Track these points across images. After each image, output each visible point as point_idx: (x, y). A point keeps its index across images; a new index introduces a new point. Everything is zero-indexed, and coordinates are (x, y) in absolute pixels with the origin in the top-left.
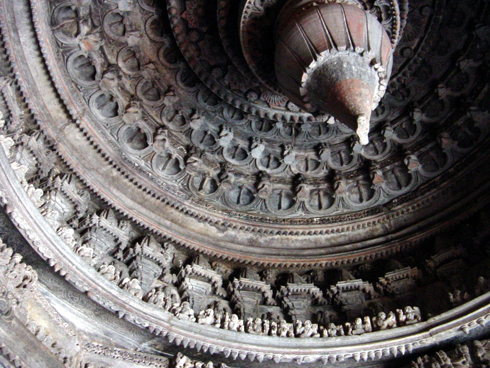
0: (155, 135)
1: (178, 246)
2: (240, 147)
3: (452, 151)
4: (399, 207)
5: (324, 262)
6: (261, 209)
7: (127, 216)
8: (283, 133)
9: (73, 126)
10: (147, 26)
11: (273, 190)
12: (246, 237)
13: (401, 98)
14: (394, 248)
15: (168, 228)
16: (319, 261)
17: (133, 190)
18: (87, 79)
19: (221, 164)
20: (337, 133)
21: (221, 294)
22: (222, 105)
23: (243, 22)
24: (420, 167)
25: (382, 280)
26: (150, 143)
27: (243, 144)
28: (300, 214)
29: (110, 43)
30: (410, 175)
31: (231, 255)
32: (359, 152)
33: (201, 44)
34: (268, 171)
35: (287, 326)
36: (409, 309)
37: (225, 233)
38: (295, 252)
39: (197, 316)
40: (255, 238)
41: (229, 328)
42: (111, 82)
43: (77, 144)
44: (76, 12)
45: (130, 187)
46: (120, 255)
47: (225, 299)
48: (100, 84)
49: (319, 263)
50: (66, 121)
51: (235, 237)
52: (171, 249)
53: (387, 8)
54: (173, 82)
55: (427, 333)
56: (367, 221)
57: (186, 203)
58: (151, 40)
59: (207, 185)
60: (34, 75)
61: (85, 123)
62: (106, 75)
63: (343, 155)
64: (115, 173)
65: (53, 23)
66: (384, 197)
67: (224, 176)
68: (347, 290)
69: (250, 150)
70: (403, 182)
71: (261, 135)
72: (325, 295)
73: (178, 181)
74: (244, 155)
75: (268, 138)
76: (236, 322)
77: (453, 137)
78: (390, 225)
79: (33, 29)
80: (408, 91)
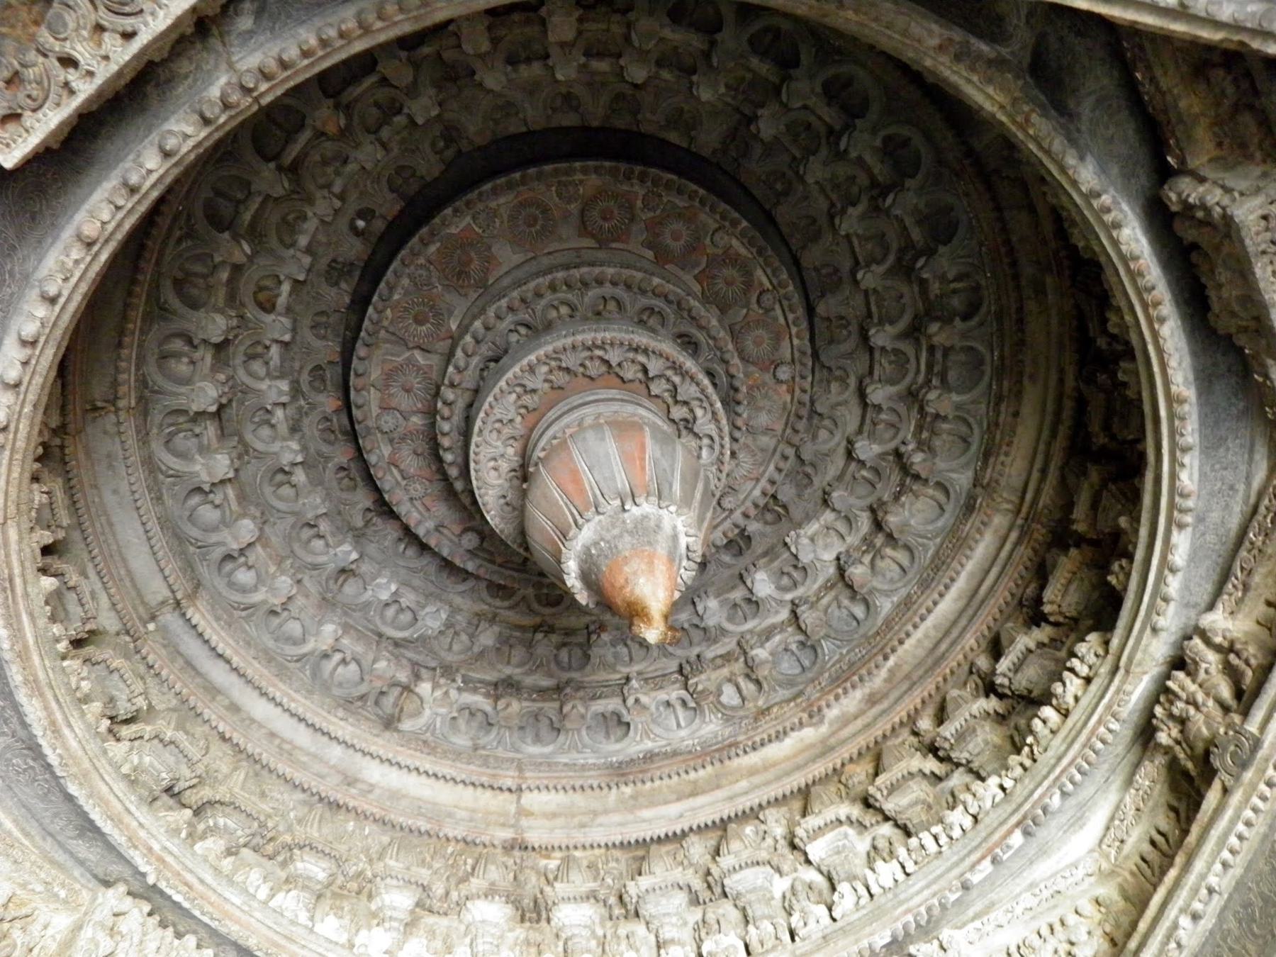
1: (777, 802)
2: (738, 601)
3: (964, 335)
4: (989, 470)
5: (972, 641)
6: (839, 647)
7: (683, 831)
10: (489, 600)
11: (826, 611)
12: (855, 702)
13: (845, 332)
14: (1036, 535)
16: (963, 648)
17: (669, 787)
18: (488, 732)
21: (873, 821)
24: (955, 398)
26: (627, 718)
28: (885, 606)
31: (851, 749)
32: (871, 454)
34: (800, 591)
36: (1081, 648)
37: (826, 721)
40: (867, 691)
42: (510, 710)
43: (552, 807)
44: (395, 684)
45: (660, 788)
49: (967, 648)
50: (514, 797)
51: (843, 714)
55: (1122, 672)
56: (973, 530)
57: (741, 738)
58: (510, 608)
59: (748, 687)
68: (1017, 668)
69: (751, 591)
71: (746, 560)
72: (1001, 696)
74: (754, 603)
75: (760, 551)
77: (947, 320)
78: (1009, 502)
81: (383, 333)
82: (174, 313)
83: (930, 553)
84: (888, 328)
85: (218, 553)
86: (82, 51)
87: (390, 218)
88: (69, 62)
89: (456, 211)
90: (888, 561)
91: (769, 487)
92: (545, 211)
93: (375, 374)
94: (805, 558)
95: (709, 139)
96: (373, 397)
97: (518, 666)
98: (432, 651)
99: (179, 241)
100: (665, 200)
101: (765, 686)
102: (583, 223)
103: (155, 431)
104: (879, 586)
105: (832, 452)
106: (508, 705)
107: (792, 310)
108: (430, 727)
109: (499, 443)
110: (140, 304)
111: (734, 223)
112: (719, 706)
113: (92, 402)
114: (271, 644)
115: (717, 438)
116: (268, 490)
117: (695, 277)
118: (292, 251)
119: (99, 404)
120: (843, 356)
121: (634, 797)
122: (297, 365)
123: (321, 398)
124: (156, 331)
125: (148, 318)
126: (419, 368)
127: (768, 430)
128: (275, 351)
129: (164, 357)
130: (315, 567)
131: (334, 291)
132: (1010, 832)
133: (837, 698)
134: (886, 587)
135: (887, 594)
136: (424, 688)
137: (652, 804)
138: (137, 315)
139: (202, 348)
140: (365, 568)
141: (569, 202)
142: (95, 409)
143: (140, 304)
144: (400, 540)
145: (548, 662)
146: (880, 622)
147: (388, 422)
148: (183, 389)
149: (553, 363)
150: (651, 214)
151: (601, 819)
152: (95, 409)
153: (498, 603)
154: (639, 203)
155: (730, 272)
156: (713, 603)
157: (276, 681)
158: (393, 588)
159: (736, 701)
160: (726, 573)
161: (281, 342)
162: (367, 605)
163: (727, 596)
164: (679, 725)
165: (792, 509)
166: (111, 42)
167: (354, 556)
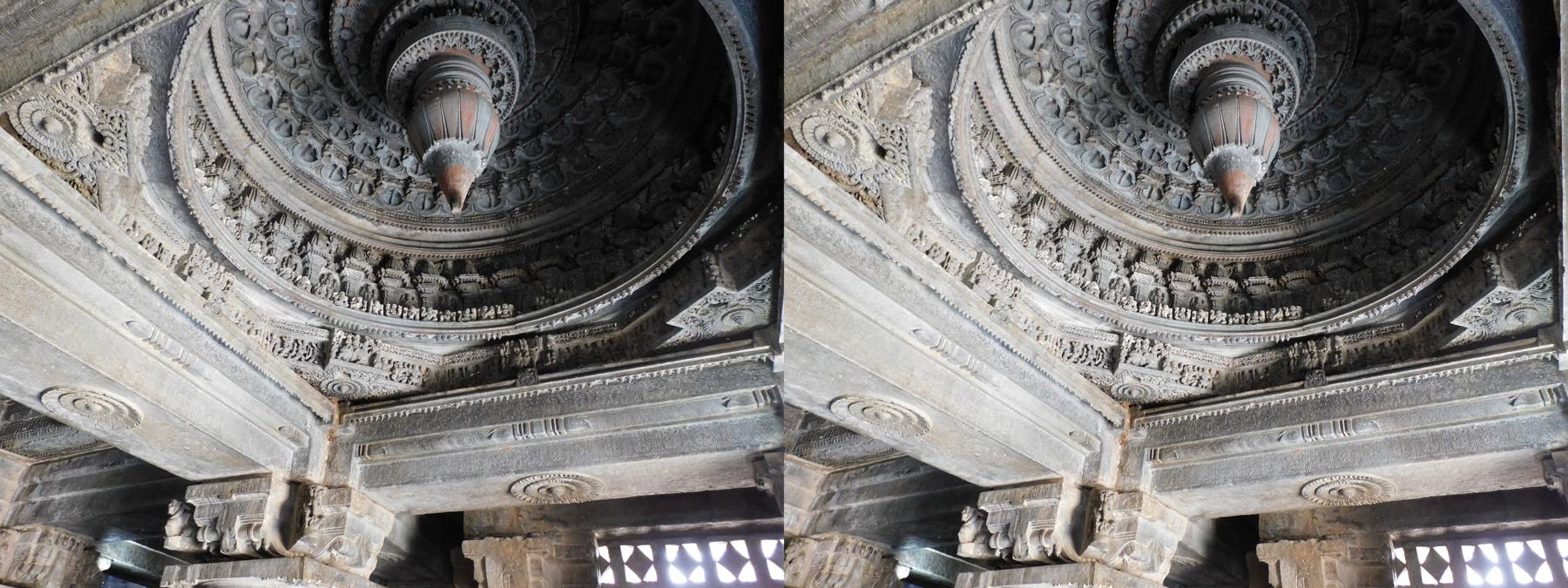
0: (323, 150)
15: (334, 225)
19: (377, 170)
25: (495, 276)
35: (415, 311)
38: (432, 245)
39: (350, 301)
41: (373, 312)
46: (296, 250)
47: (375, 282)
52: (336, 241)
54: (338, 103)
58: (318, 67)
60: (220, 107)
62: (282, 105)
64: (291, 181)
67: (378, 183)
76: (378, 306)
80: (540, 114)
101: (373, 196)
106: (286, 109)
121: (290, 186)
132: (432, 333)
137: (294, 194)
151: (273, 183)
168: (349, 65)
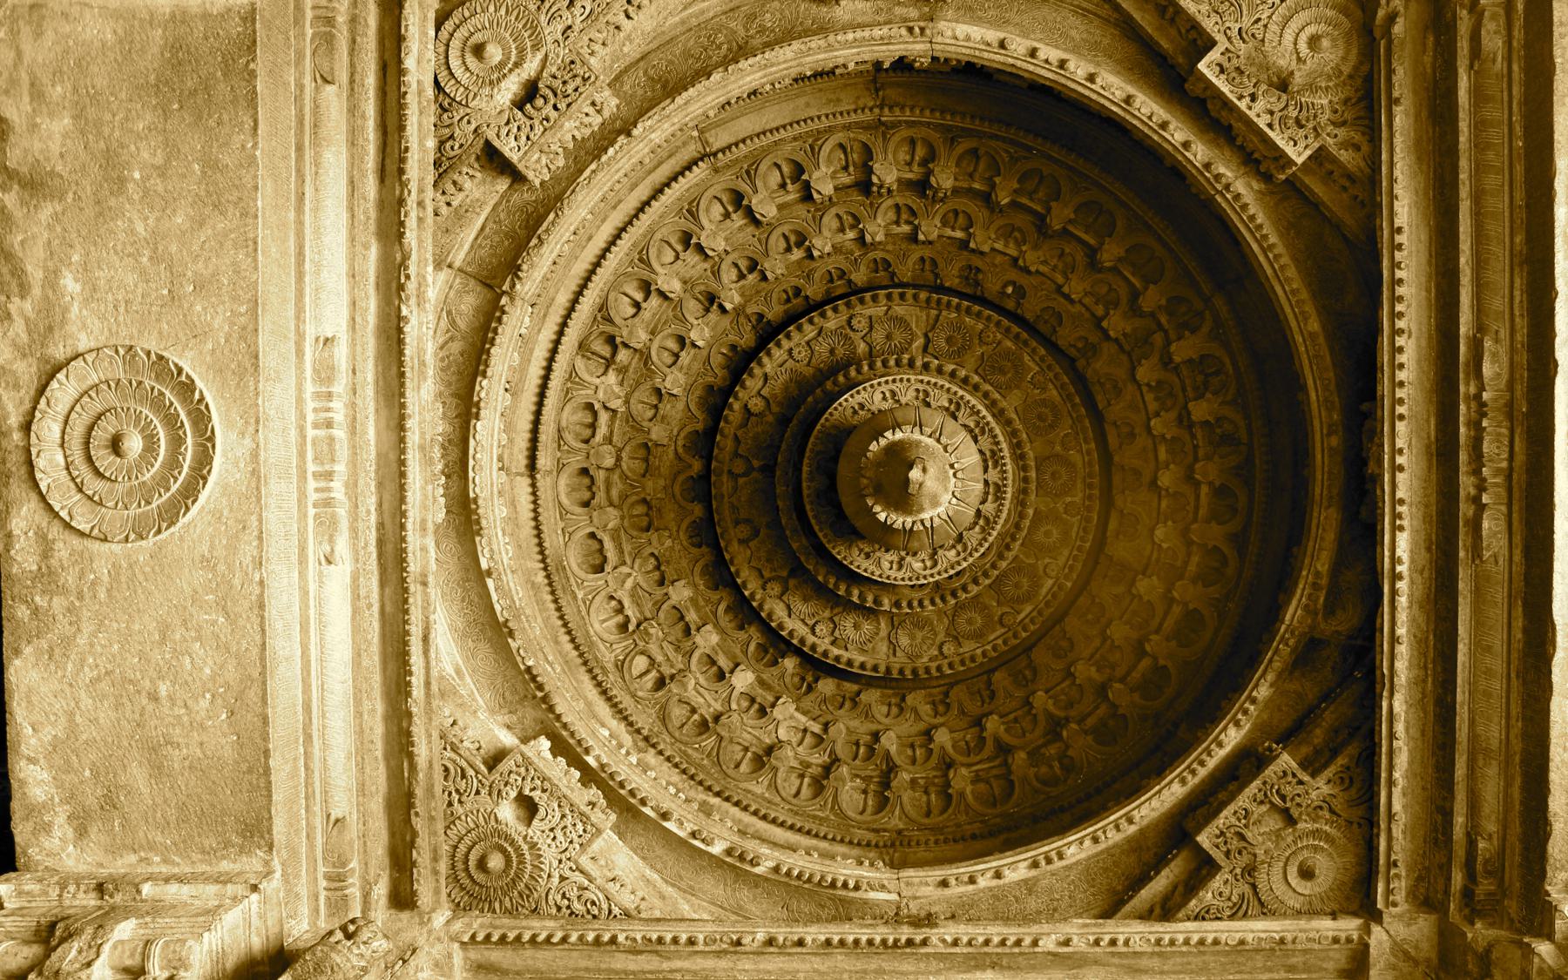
6: (709, 755)
8: (787, 680)
9: (529, 481)
10: (682, 435)
17: (548, 618)
20: (867, 716)
22: (724, 595)
23: (823, 426)
27: (723, 662)
29: (627, 421)
30: (949, 797)
33: (741, 481)
48: (592, 451)
50: (523, 470)
53: (993, 453)
61: (544, 482)
63: (862, 750)
64: (540, 578)
65: (583, 347)
66: (900, 819)
69: (732, 672)
70: (935, 811)
73: (614, 646)
74: (721, 676)
79: (561, 333)
81: (933, 312)
82: (951, 148)
83: (819, 813)
84: (1002, 728)
85: (744, 187)
86: (1260, 105)
87: (1019, 311)
88: (1253, 98)
89: (1042, 359)
90: (797, 782)
91: (844, 660)
92: (1052, 426)
93: (899, 310)
94: (777, 713)
95: (1120, 550)
96: (878, 310)
97: (629, 468)
98: (638, 384)
99: (1007, 152)
100: (1074, 519)
102: (1048, 458)
103: (852, 135)
104: (779, 774)
105: (873, 719)
107: (1005, 643)
108: (582, 383)
109: (909, 397)
110: (958, 122)
111: (1066, 577)
112: (629, 656)
113: (883, 87)
114: (658, 236)
115: (935, 571)
116: (786, 229)
117: (1016, 557)
118: (993, 236)
119: (881, 93)
120: (960, 704)
122: (890, 247)
123: (863, 268)
124: (935, 137)
125: (945, 129)
126: (910, 344)
127: (893, 647)
128: (906, 228)
129: (912, 142)
130: (716, 273)
131: (955, 272)
133: (668, 759)
134: (779, 781)
135: (773, 785)
136: (612, 378)
138: (949, 120)
139: (922, 170)
140: (714, 315)
141: (1063, 444)
142: (877, 90)
143: (958, 122)
144: (733, 347)
145: (637, 494)
146: (741, 785)
147: (860, 324)
148: (890, 156)
149: (977, 431)
150: (1061, 510)
152: (877, 90)
153: (680, 443)
154: (1069, 499)
155: (1025, 582)
156: (715, 638)
157: (632, 241)
158: (700, 343)
159: (635, 673)
160: (738, 651)
161: (917, 234)
162: (683, 320)
163: (720, 652)
164: (604, 621)
165: (811, 696)
166: (1266, 118)
167: (728, 306)
168: (736, 455)
